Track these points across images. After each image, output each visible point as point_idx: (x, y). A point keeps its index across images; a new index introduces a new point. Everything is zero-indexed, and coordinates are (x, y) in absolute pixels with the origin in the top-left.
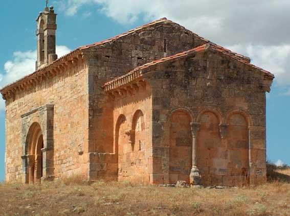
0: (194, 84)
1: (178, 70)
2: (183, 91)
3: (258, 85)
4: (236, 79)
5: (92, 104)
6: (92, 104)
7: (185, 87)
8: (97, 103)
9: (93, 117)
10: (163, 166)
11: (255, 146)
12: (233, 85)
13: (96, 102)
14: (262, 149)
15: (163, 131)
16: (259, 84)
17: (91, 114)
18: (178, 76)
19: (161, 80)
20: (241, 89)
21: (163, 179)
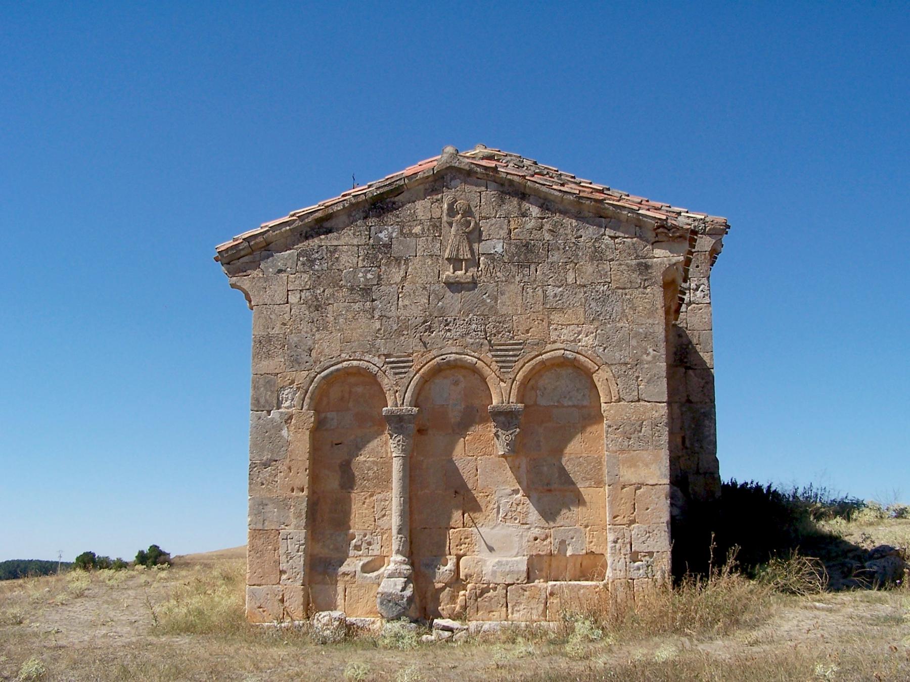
0: (398, 280)
2: (356, 306)
3: (634, 262)
10: (283, 558)
15: (289, 443)
18: (344, 259)
20: (570, 279)
21: (282, 601)
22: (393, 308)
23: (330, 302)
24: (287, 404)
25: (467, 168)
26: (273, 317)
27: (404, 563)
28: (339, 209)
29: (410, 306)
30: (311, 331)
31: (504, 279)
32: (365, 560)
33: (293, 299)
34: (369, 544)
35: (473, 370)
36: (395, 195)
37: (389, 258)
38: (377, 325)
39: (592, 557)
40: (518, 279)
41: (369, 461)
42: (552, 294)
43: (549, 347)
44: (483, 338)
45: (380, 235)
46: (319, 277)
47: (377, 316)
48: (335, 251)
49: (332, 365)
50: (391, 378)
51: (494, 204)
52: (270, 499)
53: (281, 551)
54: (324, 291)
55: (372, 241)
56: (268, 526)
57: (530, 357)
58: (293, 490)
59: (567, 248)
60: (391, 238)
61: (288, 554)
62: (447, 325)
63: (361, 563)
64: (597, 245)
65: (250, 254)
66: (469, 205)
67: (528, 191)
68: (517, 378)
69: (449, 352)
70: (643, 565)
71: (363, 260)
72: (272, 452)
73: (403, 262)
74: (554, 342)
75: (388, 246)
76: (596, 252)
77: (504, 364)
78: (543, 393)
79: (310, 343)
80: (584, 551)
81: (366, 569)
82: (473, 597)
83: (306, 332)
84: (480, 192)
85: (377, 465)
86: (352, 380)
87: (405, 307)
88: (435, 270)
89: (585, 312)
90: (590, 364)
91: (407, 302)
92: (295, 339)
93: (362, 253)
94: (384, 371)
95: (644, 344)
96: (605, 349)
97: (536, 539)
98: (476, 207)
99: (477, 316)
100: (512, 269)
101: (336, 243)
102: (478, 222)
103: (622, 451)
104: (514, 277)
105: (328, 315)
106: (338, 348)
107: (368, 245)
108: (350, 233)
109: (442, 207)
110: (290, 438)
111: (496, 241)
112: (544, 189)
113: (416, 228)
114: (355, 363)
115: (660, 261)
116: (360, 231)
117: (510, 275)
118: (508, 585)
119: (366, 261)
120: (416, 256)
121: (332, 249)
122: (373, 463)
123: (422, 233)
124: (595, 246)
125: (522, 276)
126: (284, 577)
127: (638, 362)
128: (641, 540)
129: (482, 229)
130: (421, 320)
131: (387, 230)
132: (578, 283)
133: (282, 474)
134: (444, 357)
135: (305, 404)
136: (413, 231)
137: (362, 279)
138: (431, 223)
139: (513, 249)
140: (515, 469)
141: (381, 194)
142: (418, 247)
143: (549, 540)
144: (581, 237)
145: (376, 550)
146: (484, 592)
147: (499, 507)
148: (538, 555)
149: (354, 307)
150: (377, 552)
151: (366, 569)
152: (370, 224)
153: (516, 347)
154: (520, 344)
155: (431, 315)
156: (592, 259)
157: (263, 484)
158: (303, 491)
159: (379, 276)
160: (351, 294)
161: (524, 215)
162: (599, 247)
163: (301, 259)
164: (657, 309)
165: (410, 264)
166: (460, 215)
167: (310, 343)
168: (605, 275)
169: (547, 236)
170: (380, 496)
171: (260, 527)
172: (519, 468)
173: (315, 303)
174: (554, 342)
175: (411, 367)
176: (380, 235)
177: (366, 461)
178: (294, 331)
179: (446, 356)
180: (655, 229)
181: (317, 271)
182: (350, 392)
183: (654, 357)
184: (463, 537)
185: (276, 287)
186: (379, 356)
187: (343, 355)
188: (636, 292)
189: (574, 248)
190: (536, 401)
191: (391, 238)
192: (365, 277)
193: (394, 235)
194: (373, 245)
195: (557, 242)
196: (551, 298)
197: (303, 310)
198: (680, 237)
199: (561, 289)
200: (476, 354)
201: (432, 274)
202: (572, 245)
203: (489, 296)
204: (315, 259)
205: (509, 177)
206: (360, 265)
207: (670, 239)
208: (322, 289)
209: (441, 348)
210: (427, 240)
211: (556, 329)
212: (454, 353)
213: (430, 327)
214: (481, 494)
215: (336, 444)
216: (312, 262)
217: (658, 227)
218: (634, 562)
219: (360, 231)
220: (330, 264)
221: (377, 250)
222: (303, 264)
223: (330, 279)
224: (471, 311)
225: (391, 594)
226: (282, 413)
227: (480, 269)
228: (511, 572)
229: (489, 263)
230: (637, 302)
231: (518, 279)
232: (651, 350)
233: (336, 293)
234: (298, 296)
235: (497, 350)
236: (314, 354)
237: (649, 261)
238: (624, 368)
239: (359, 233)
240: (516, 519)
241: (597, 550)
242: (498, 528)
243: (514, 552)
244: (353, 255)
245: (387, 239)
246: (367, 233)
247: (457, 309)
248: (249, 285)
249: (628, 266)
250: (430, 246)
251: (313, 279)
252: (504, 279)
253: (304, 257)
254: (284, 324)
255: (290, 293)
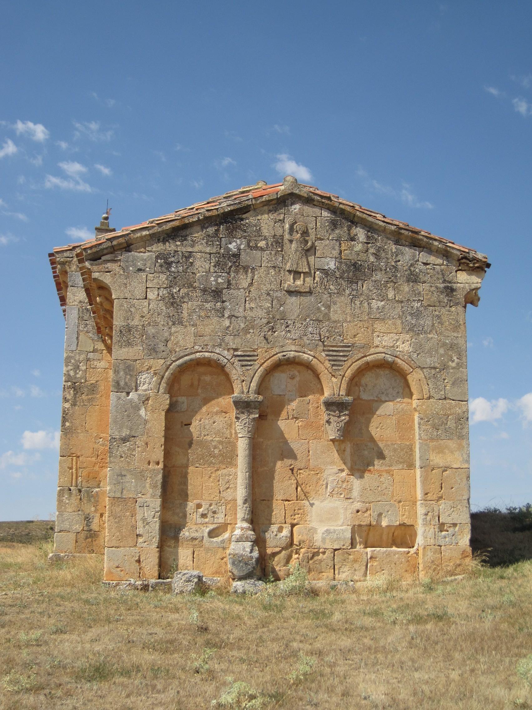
0: (245, 284)
1: (196, 249)
2: (208, 305)
3: (442, 286)
4: (373, 269)
5: (72, 373)
6: (72, 373)
7: (217, 294)
8: (85, 371)
9: (74, 404)
10: (140, 524)
11: (437, 459)
12: (366, 287)
13: (84, 368)
14: (455, 466)
15: (146, 422)
16: (445, 281)
17: (68, 397)
18: (198, 264)
19: (143, 275)
20: (391, 295)
21: (139, 561)
22: (241, 310)
23: (185, 300)
24: (145, 387)
25: (305, 195)
26: (132, 309)
27: (248, 529)
28: (194, 220)
29: (255, 309)
30: (168, 324)
31: (336, 291)
32: (211, 527)
33: (152, 295)
34: (214, 512)
35: (308, 366)
36: (242, 213)
37: (238, 266)
38: (227, 323)
39: (403, 528)
40: (347, 292)
41: (215, 440)
42: (376, 306)
43: (372, 350)
44: (318, 340)
45: (229, 246)
46: (175, 278)
47: (226, 315)
48: (190, 257)
49: (186, 355)
50: (238, 368)
51: (328, 228)
52: (129, 471)
53: (139, 517)
54: (179, 291)
55: (222, 251)
56: (126, 495)
57: (357, 358)
58: (149, 463)
59: (388, 270)
60: (239, 249)
61: (144, 520)
62: (288, 326)
63: (208, 530)
64: (412, 269)
65: (112, 253)
66: (307, 227)
67: (356, 219)
68: (346, 375)
69: (289, 350)
70: (448, 534)
71: (215, 266)
72: (131, 430)
73: (250, 271)
74: (377, 346)
75: (237, 256)
76: (411, 275)
77: (336, 362)
78: (364, 389)
79: (166, 334)
80: (398, 523)
81: (212, 534)
82: (306, 560)
83: (163, 325)
84: (316, 217)
85: (222, 444)
86: (201, 369)
87: (251, 309)
88: (278, 280)
89: (402, 323)
90: (405, 366)
91: (253, 305)
92: (153, 331)
93: (213, 260)
94: (232, 362)
95: (450, 353)
96: (418, 354)
97: (358, 511)
98: (312, 229)
99: (313, 320)
100: (343, 284)
101: (190, 249)
102: (314, 242)
103: (432, 439)
104: (344, 290)
105: (183, 312)
106: (192, 340)
107: (219, 253)
108: (203, 242)
109: (283, 227)
110: (147, 418)
111: (329, 259)
112: (370, 219)
113: (261, 243)
114: (207, 354)
115: (462, 286)
116: (212, 241)
117: (341, 289)
118: (335, 550)
119: (217, 267)
120: (261, 266)
121: (187, 254)
122: (219, 443)
123: (267, 248)
124: (410, 270)
125: (351, 290)
126: (140, 540)
127: (445, 367)
128: (447, 514)
129: (317, 248)
130: (265, 321)
131: (236, 242)
132: (397, 299)
133: (140, 449)
134: (284, 353)
135: (161, 388)
136: (259, 245)
137: (214, 283)
138: (274, 240)
139: (344, 267)
140: (341, 452)
141: (231, 211)
142: (264, 259)
143: (369, 512)
144: (399, 261)
145: (220, 518)
146: (317, 554)
147: (327, 484)
148: (360, 526)
149: (207, 306)
150: (221, 520)
151: (212, 534)
152: (221, 236)
153: (346, 349)
154: (349, 347)
155: (274, 318)
156: (408, 281)
157: (121, 457)
158: (158, 463)
159: (229, 281)
160: (204, 294)
161: (353, 239)
162: (414, 271)
163: (159, 261)
164: (460, 324)
165: (256, 273)
166: (299, 235)
167: (166, 334)
168: (418, 294)
169: (372, 259)
170: (224, 471)
171: (118, 495)
172: (344, 451)
173: (171, 300)
174: (377, 346)
175: (255, 361)
176: (229, 246)
177: (212, 440)
178: (152, 324)
179: (287, 353)
180: (459, 260)
181: (174, 272)
182: (199, 380)
183: (458, 364)
184: (297, 508)
185: (136, 284)
186: (228, 350)
187: (196, 347)
188: (443, 310)
189: (394, 270)
190: (359, 396)
191: (239, 249)
192: (216, 281)
193: (242, 247)
194: (223, 254)
195: (379, 264)
196: (375, 310)
197: (160, 305)
198: (478, 267)
199: (383, 303)
200: (312, 353)
201: (275, 283)
202: (392, 268)
203: (323, 305)
204: (172, 262)
205: (341, 206)
206: (212, 270)
207: (471, 269)
208: (178, 289)
209: (282, 346)
210: (271, 253)
211: (378, 336)
212: (293, 351)
213: (273, 328)
214: (312, 472)
215: (185, 425)
216: (169, 264)
217: (462, 258)
218: (441, 531)
219: (212, 241)
220: (185, 267)
221: (227, 258)
222: (161, 266)
223: (185, 280)
224: (308, 316)
225: (242, 555)
226: (139, 395)
227: (315, 281)
228: (338, 539)
229: (324, 277)
230: (444, 318)
231: (347, 292)
232: (455, 358)
233: (190, 293)
234: (156, 293)
235: (330, 351)
236: (170, 344)
237: (455, 286)
238: (433, 371)
239: (211, 243)
240: (341, 494)
241: (408, 522)
242: (326, 502)
243: (340, 522)
244: (205, 261)
245: (236, 250)
246: (217, 243)
247: (296, 314)
248: (110, 280)
249: (437, 287)
250: (274, 259)
251: (170, 279)
252: (336, 291)
253: (161, 260)
254: (143, 317)
255: (148, 290)
